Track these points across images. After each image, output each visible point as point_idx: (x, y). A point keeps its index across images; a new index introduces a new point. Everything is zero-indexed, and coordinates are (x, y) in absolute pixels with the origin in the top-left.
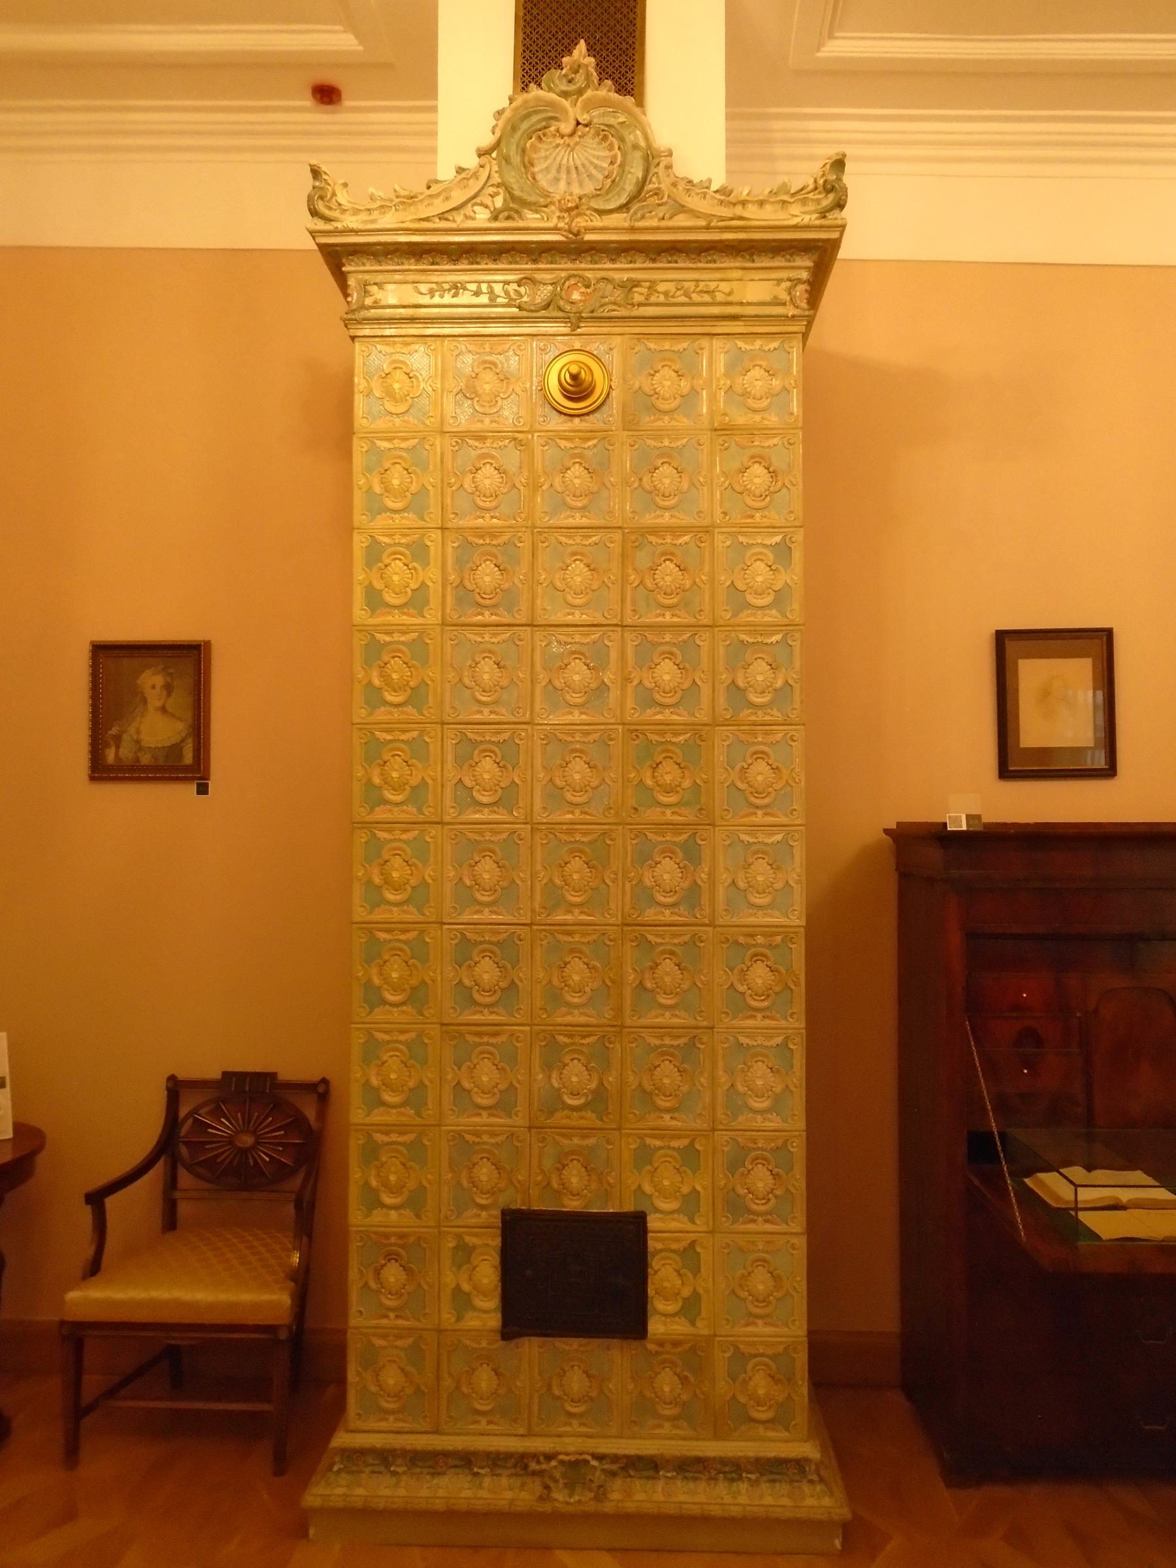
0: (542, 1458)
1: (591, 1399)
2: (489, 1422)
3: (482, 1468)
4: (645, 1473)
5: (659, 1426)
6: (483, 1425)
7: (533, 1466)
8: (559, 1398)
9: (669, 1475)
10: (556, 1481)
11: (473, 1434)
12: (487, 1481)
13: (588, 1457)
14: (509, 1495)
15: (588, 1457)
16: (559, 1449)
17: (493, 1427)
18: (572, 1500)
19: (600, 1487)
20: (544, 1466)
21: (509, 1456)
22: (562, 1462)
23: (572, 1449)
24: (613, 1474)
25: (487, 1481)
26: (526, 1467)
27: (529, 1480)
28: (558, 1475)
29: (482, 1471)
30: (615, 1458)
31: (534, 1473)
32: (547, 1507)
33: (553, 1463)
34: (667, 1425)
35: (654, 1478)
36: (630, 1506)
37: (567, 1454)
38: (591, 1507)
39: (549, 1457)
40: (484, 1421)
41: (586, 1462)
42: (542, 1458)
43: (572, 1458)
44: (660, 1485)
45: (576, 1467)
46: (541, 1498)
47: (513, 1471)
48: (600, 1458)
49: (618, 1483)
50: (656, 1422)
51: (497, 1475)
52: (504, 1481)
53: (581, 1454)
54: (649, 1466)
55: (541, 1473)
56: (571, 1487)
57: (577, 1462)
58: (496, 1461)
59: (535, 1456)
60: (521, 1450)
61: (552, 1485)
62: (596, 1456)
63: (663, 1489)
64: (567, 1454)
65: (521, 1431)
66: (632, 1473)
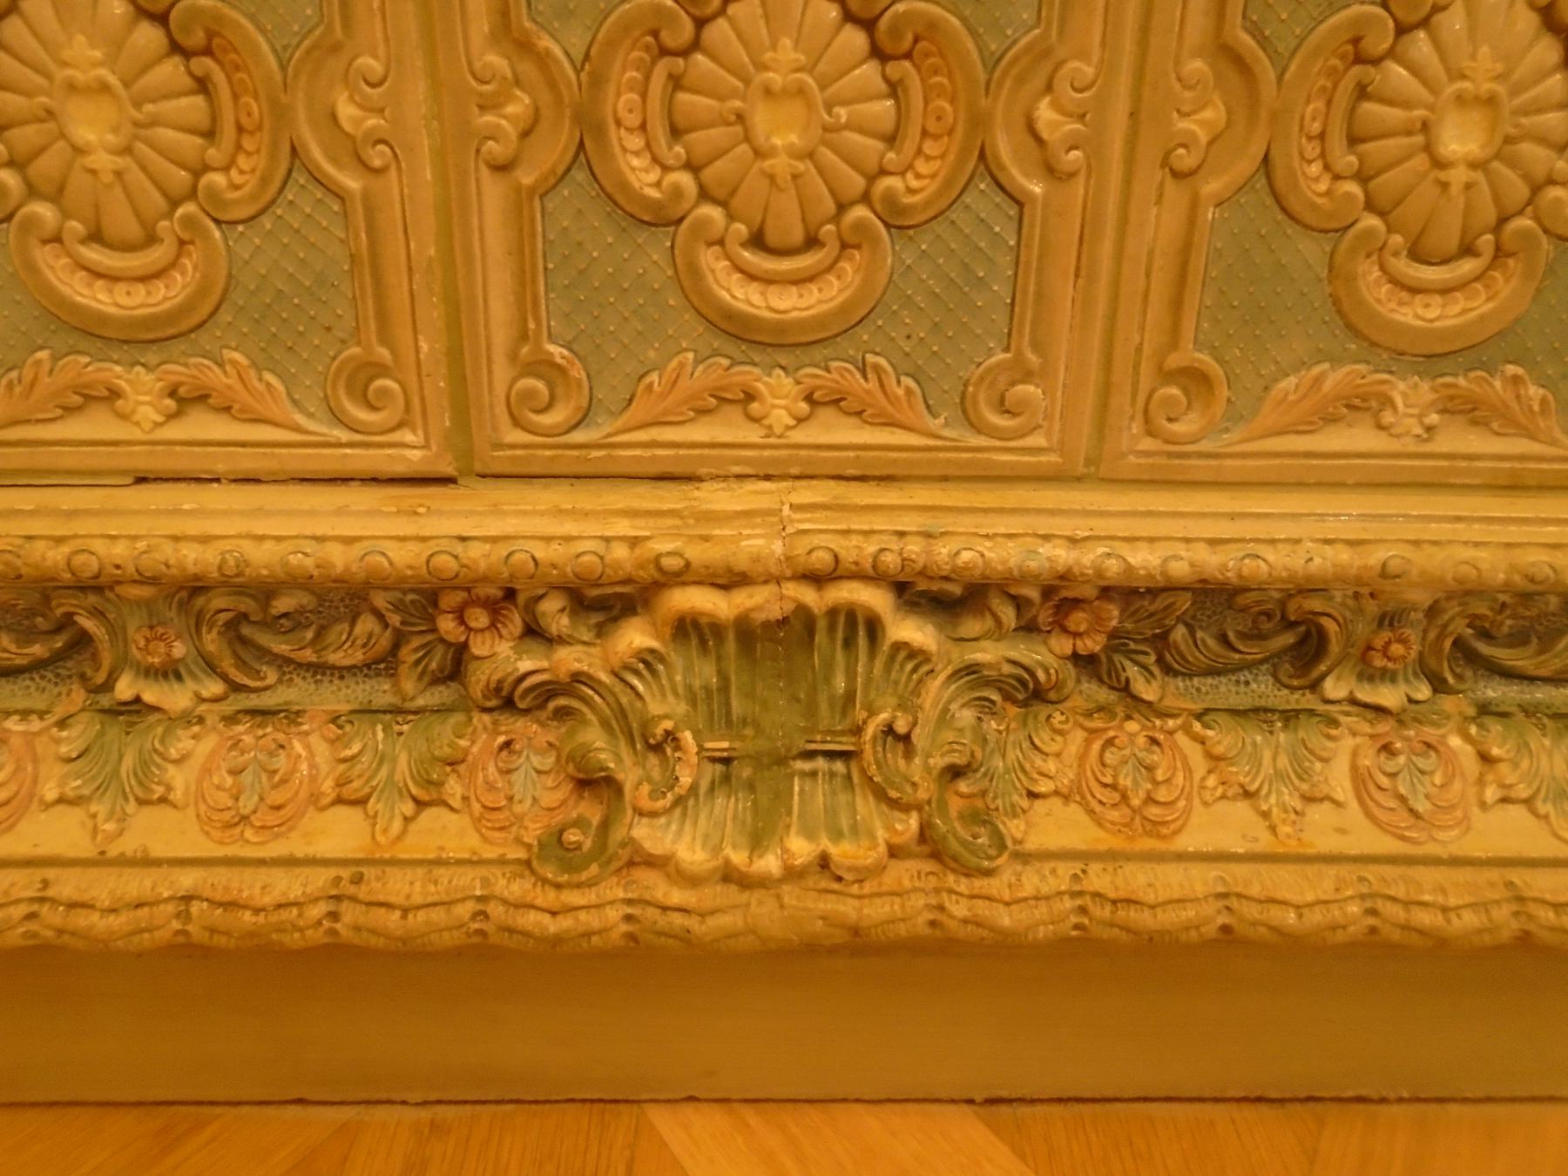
0: (553, 611)
1: (897, 219)
2: (185, 400)
3: (170, 672)
4: (1227, 692)
5: (1363, 405)
6: (143, 408)
7: (502, 656)
8: (661, 219)
9: (1389, 696)
10: (661, 746)
11: (91, 477)
12: (196, 758)
13: (876, 599)
14: (339, 833)
15: (876, 599)
16: (665, 546)
17: (203, 426)
18: (770, 863)
19: (955, 772)
20: (569, 659)
21: (342, 597)
22: (688, 629)
23: (757, 545)
24: (1031, 693)
25: (196, 758)
26: (457, 664)
27: (479, 736)
28: (662, 707)
29: (176, 698)
30: (1053, 601)
31: (505, 700)
32: (599, 908)
33: (635, 636)
34: (1410, 394)
35: (1290, 717)
36: (1172, 893)
37: (730, 580)
38: (903, 900)
39: (604, 601)
40: (143, 387)
41: (860, 628)
42: (553, 611)
43: (759, 601)
44: (1343, 753)
45: (790, 646)
46: (557, 854)
47: (380, 692)
48: (949, 598)
49: (1062, 747)
50: (1335, 378)
51: (262, 714)
52: (311, 754)
53: (817, 579)
54: (1279, 638)
55: (550, 698)
56: (751, 775)
57: (800, 626)
58: (256, 628)
59: (507, 598)
60: (405, 557)
61: (630, 772)
62: (925, 594)
63: (1360, 779)
64: (730, 580)
65: (412, 453)
66: (1147, 690)
